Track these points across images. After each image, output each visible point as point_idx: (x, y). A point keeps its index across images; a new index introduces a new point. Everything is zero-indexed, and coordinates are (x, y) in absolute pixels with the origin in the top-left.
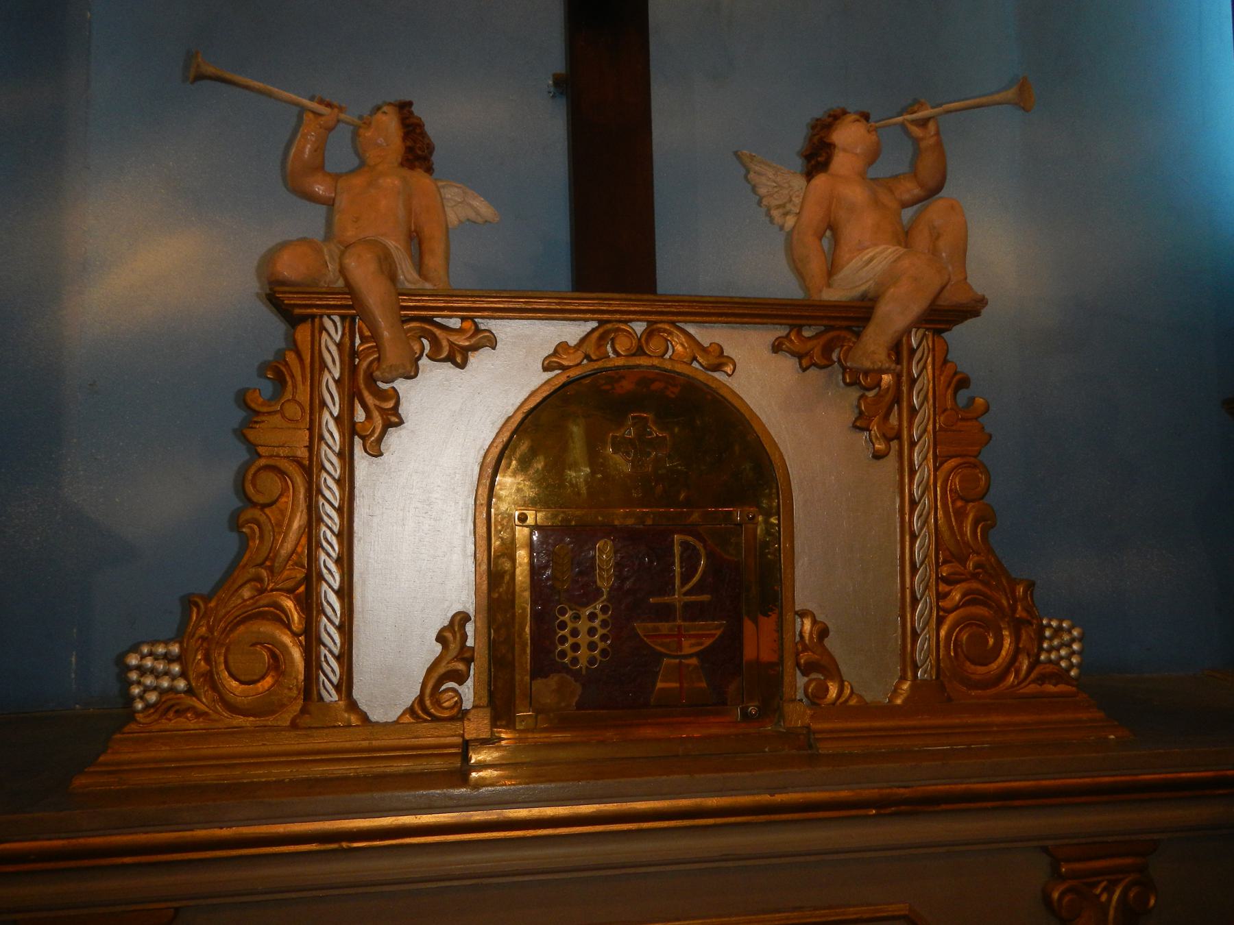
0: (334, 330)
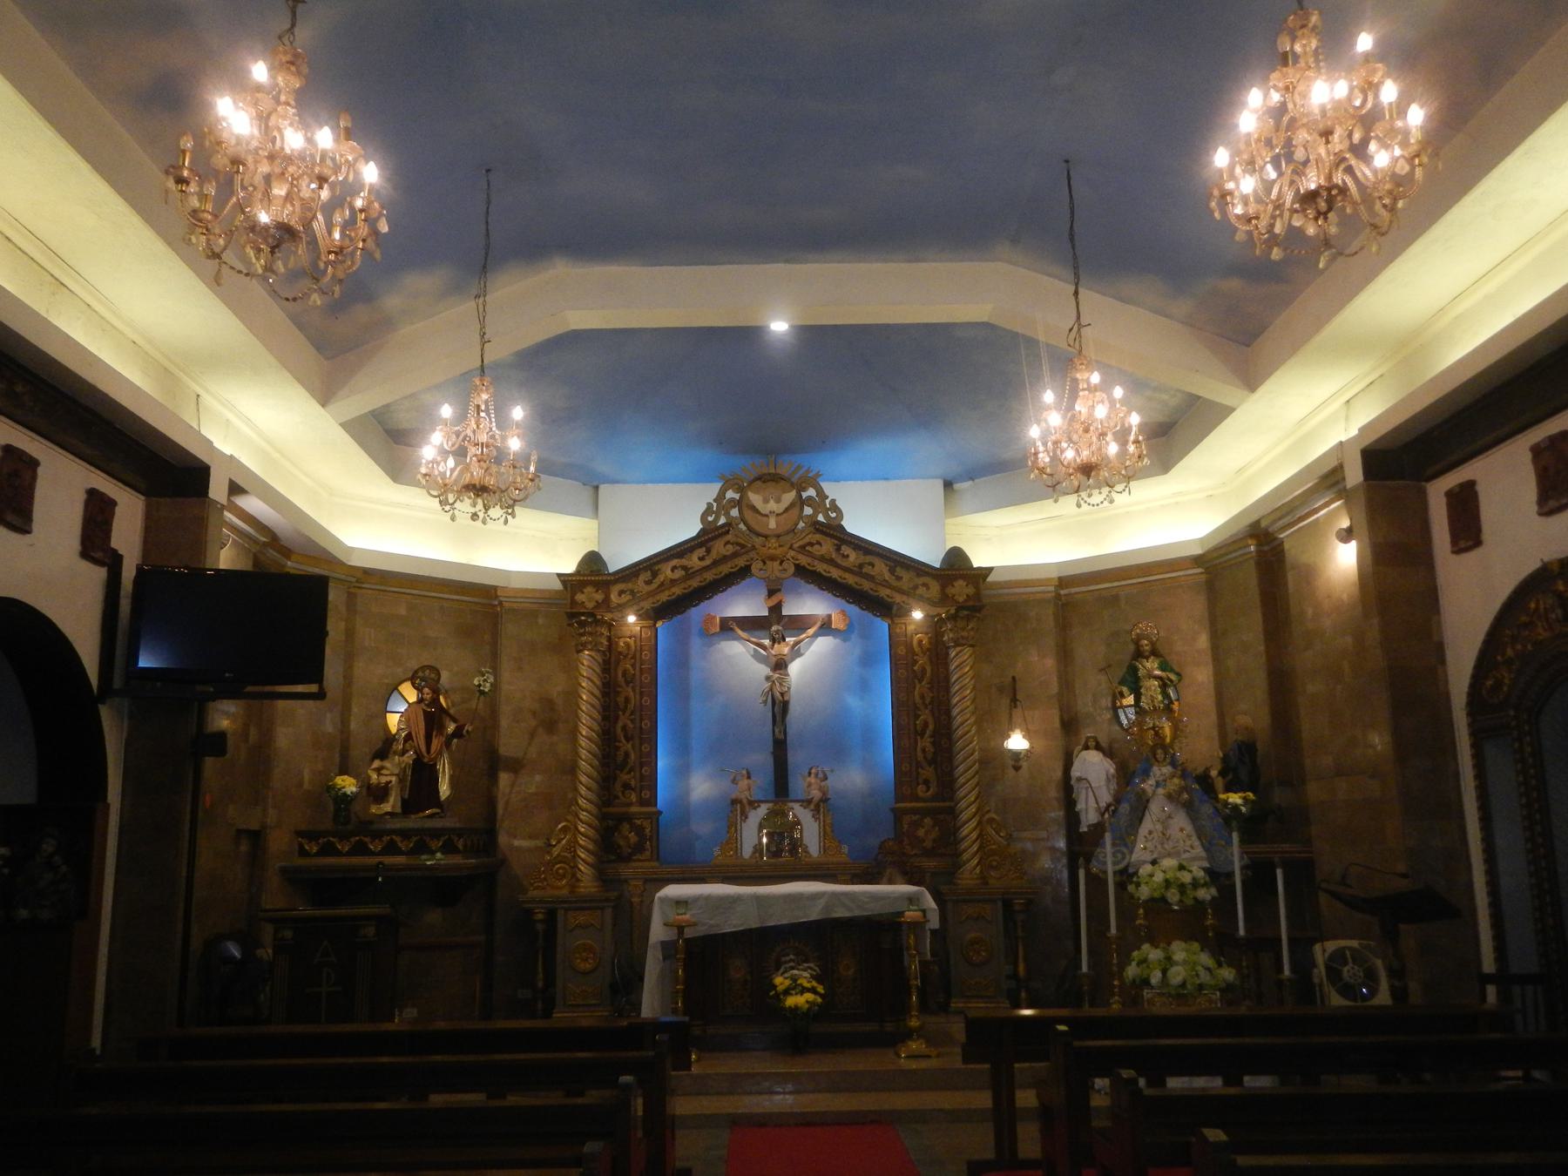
0: (739, 805)
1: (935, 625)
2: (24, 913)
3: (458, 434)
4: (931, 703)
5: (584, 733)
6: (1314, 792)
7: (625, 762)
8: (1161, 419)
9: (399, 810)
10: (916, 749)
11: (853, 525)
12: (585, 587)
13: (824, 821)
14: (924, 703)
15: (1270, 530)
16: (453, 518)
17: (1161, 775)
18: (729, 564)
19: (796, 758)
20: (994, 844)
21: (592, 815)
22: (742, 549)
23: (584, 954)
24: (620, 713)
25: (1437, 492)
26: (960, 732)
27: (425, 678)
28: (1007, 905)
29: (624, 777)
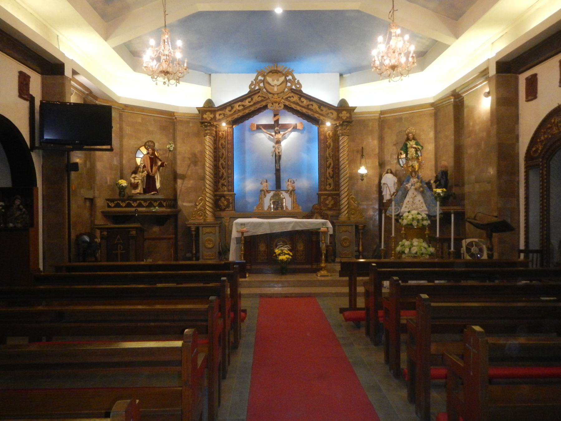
1: (335, 128)
2: (11, 225)
3: (157, 51)
4: (332, 156)
5: (207, 166)
6: (467, 189)
7: (222, 176)
8: (422, 50)
9: (142, 192)
10: (326, 173)
11: (306, 90)
12: (207, 112)
13: (293, 198)
14: (330, 156)
15: (460, 93)
16: (157, 84)
17: (414, 181)
18: (260, 104)
19: (283, 175)
20: (353, 206)
21: (211, 195)
22: (265, 99)
23: (209, 242)
24: (221, 159)
25: (523, 78)
26: (342, 167)
27: (149, 145)
28: (357, 227)
29: (222, 181)
